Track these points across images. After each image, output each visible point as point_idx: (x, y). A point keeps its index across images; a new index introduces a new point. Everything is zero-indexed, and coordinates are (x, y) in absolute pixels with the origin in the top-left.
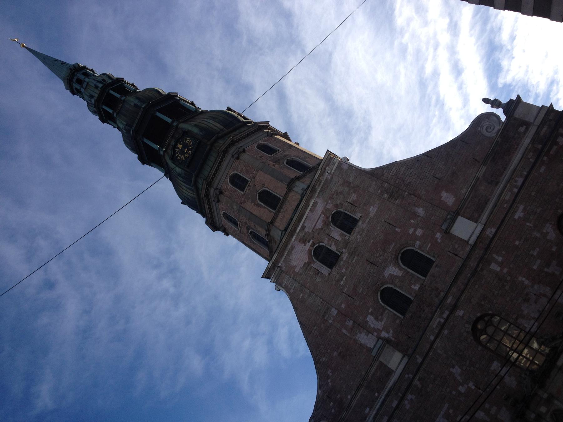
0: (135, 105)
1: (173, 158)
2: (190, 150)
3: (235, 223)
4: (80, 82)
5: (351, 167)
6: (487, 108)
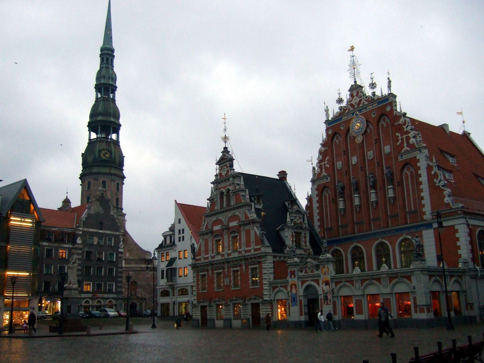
0: (111, 113)
1: (100, 151)
2: (106, 158)
3: (89, 188)
4: (107, 59)
5: (125, 224)
6: (152, 253)
